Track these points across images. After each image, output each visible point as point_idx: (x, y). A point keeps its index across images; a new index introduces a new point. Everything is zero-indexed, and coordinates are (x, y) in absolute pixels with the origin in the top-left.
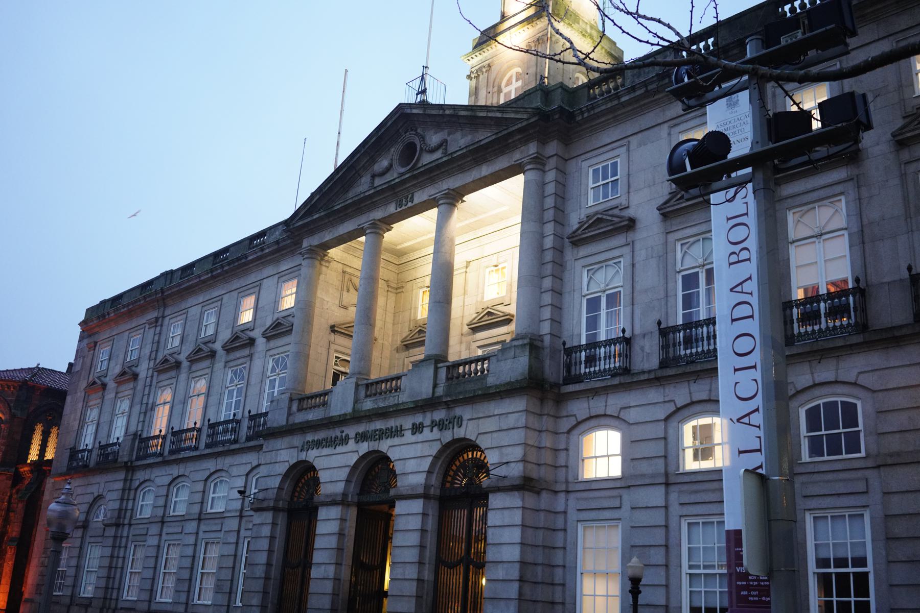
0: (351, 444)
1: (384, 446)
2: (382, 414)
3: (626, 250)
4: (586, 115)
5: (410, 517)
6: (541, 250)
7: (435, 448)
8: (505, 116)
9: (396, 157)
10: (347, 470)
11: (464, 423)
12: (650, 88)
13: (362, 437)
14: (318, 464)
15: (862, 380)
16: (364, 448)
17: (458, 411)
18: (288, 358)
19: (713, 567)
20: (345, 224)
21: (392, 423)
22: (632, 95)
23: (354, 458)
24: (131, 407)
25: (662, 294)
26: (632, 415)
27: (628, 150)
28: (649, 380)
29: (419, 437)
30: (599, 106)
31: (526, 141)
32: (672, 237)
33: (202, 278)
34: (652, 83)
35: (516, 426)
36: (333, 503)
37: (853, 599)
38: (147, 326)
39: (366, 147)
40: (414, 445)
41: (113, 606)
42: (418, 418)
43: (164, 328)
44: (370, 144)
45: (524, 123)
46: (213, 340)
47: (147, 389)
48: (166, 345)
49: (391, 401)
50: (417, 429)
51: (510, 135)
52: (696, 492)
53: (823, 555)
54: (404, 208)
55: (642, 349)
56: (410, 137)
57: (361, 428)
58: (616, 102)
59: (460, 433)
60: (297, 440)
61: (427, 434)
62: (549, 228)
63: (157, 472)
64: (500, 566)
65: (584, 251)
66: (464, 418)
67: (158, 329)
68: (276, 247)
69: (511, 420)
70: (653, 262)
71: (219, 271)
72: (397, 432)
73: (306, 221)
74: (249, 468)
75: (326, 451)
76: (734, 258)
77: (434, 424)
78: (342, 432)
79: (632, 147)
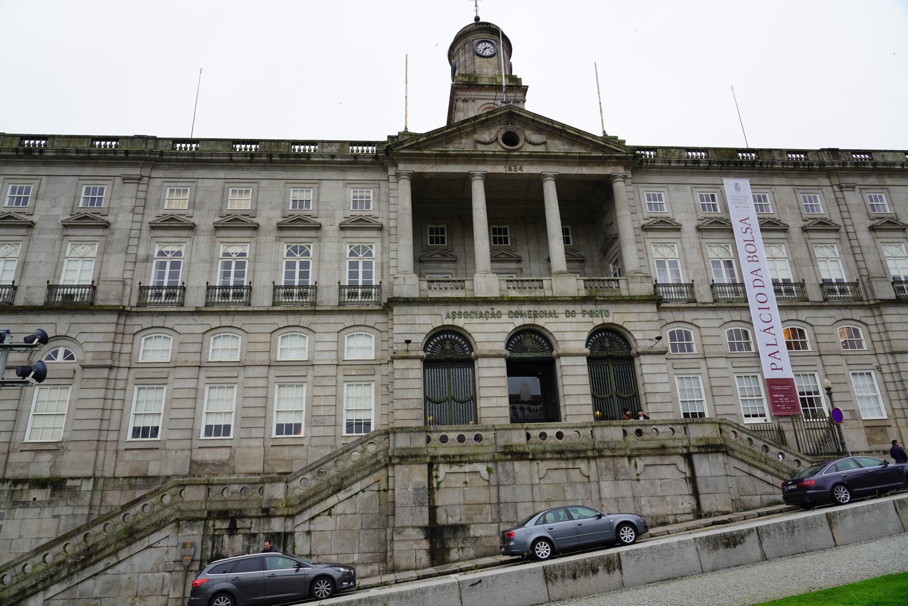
0: (505, 318)
1: (540, 322)
3: (678, 241)
4: (649, 164)
5: (577, 367)
7: (590, 328)
8: (607, 145)
9: (500, 138)
10: (506, 335)
11: (611, 315)
12: (688, 165)
13: (511, 314)
14: (468, 328)
15: (808, 320)
16: (519, 322)
17: (605, 307)
18: (290, 246)
19: (746, 396)
20: (451, 166)
22: (677, 165)
23: (511, 328)
24: (103, 252)
25: (704, 268)
26: (700, 323)
27: (668, 190)
28: (710, 307)
29: (574, 319)
30: (658, 162)
31: (617, 164)
33: (196, 158)
34: (689, 163)
35: (652, 320)
37: (809, 408)
39: (476, 121)
40: (569, 324)
41: (111, 447)
42: (571, 308)
43: (151, 188)
44: (479, 120)
45: (624, 155)
47: (134, 242)
48: (159, 203)
49: (538, 293)
50: (568, 314)
51: (610, 158)
52: (741, 362)
53: (801, 391)
54: (513, 172)
55: (699, 291)
56: (510, 128)
57: (514, 308)
58: (667, 164)
59: (609, 320)
60: (443, 310)
63: (171, 322)
64: (657, 395)
65: (650, 234)
66: (610, 311)
67: (142, 187)
68: (353, 159)
69: (648, 317)
70: (695, 251)
71: (265, 158)
72: (553, 314)
73: (411, 152)
74: (341, 327)
75: (475, 320)
76: (750, 259)
77: (584, 313)
78: (493, 309)
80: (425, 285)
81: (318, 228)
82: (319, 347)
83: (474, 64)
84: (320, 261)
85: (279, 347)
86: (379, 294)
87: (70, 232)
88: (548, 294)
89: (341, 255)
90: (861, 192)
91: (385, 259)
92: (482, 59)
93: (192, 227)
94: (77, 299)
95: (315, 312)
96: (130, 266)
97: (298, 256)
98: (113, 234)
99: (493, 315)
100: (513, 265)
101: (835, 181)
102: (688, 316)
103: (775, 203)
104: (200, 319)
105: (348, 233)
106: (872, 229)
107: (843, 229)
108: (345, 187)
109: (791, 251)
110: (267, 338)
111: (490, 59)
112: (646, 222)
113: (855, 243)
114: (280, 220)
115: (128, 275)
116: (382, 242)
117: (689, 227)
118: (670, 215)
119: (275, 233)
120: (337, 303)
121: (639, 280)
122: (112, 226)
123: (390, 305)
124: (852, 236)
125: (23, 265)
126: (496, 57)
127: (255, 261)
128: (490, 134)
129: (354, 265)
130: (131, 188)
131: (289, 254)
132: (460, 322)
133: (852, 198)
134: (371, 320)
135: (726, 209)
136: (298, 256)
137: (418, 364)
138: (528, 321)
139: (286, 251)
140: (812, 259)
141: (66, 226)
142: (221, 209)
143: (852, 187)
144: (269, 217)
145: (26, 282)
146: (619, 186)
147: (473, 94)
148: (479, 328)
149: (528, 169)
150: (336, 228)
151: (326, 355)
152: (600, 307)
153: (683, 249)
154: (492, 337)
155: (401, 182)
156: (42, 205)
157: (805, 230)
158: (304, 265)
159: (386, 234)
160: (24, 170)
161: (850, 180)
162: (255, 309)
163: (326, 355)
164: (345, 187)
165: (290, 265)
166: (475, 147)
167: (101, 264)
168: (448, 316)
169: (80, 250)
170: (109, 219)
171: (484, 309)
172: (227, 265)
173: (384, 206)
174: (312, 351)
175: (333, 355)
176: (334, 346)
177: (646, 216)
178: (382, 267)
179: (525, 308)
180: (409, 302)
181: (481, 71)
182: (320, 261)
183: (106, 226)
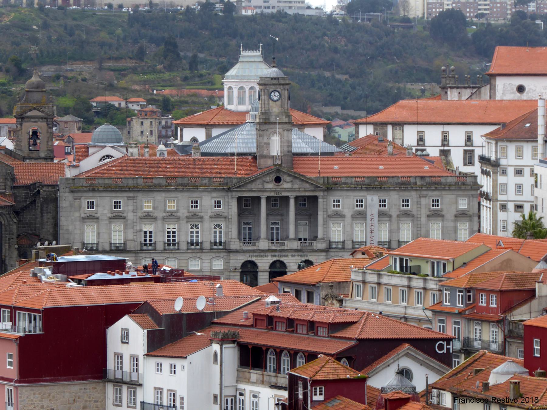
0: (269, 257)
1: (282, 259)
2: (281, 251)
6: (324, 218)
9: (274, 179)
14: (256, 261)
21: (284, 254)
23: (271, 261)
24: (125, 228)
27: (343, 199)
32: (354, 221)
36: (266, 271)
38: (126, 198)
42: (294, 254)
46: (177, 211)
47: (135, 224)
48: (142, 208)
49: (282, 248)
50: (293, 256)
57: (273, 254)
59: (307, 258)
60: (248, 254)
61: (296, 257)
62: (325, 213)
65: (332, 219)
67: (135, 201)
74: (211, 257)
75: (259, 258)
77: (298, 256)
79: (344, 198)
80: (242, 244)
81: (202, 218)
82: (204, 265)
83: (269, 104)
85: (190, 264)
86: (225, 246)
87: (112, 220)
88: (286, 248)
89: (210, 230)
90: (429, 198)
91: (227, 230)
92: (273, 102)
93: (155, 218)
94: (120, 248)
95: (202, 252)
96: (135, 234)
97: (195, 228)
98: (127, 221)
99: (265, 256)
100: (279, 217)
101: (419, 193)
103: (389, 204)
104: (162, 254)
105: (213, 219)
106: (428, 216)
107: (416, 216)
108: (211, 199)
109: (390, 226)
110: (185, 261)
111: (277, 103)
112: (331, 213)
113: (419, 223)
114: (187, 214)
115: (135, 237)
116: (226, 223)
118: (342, 210)
119: (186, 220)
120: (209, 249)
121: (321, 242)
122: (127, 218)
123: (230, 251)
124: (419, 219)
125: (99, 234)
126: (280, 100)
127: (179, 231)
128: (270, 177)
129: (215, 232)
130: (131, 202)
131: (191, 228)
132: (253, 259)
133: (424, 201)
134: (222, 255)
135: (366, 207)
136: (195, 228)
137: (239, 274)
138: (278, 259)
139: (190, 227)
140: (399, 229)
141: (110, 218)
142: (165, 210)
143: (425, 196)
144: (183, 213)
145: (101, 241)
146: (320, 200)
147: (267, 126)
148: (260, 261)
149: (284, 194)
150: (209, 217)
151: (206, 268)
152: (304, 254)
153: (345, 225)
154: (265, 265)
155: (233, 200)
156: (100, 209)
157: (398, 216)
158: (197, 232)
159: (227, 219)
160: (90, 195)
161: (425, 193)
162: (182, 251)
163: (206, 268)
164: (211, 199)
165: (192, 232)
166: (263, 185)
167: (125, 233)
168: (249, 257)
169: (117, 228)
170: (125, 215)
171: (262, 254)
172: (169, 233)
173: (226, 207)
174: (202, 266)
175: (209, 268)
176: (209, 265)
177: (331, 210)
178: (226, 234)
179: (277, 254)
180: (237, 251)
181: (272, 110)
183: (124, 218)
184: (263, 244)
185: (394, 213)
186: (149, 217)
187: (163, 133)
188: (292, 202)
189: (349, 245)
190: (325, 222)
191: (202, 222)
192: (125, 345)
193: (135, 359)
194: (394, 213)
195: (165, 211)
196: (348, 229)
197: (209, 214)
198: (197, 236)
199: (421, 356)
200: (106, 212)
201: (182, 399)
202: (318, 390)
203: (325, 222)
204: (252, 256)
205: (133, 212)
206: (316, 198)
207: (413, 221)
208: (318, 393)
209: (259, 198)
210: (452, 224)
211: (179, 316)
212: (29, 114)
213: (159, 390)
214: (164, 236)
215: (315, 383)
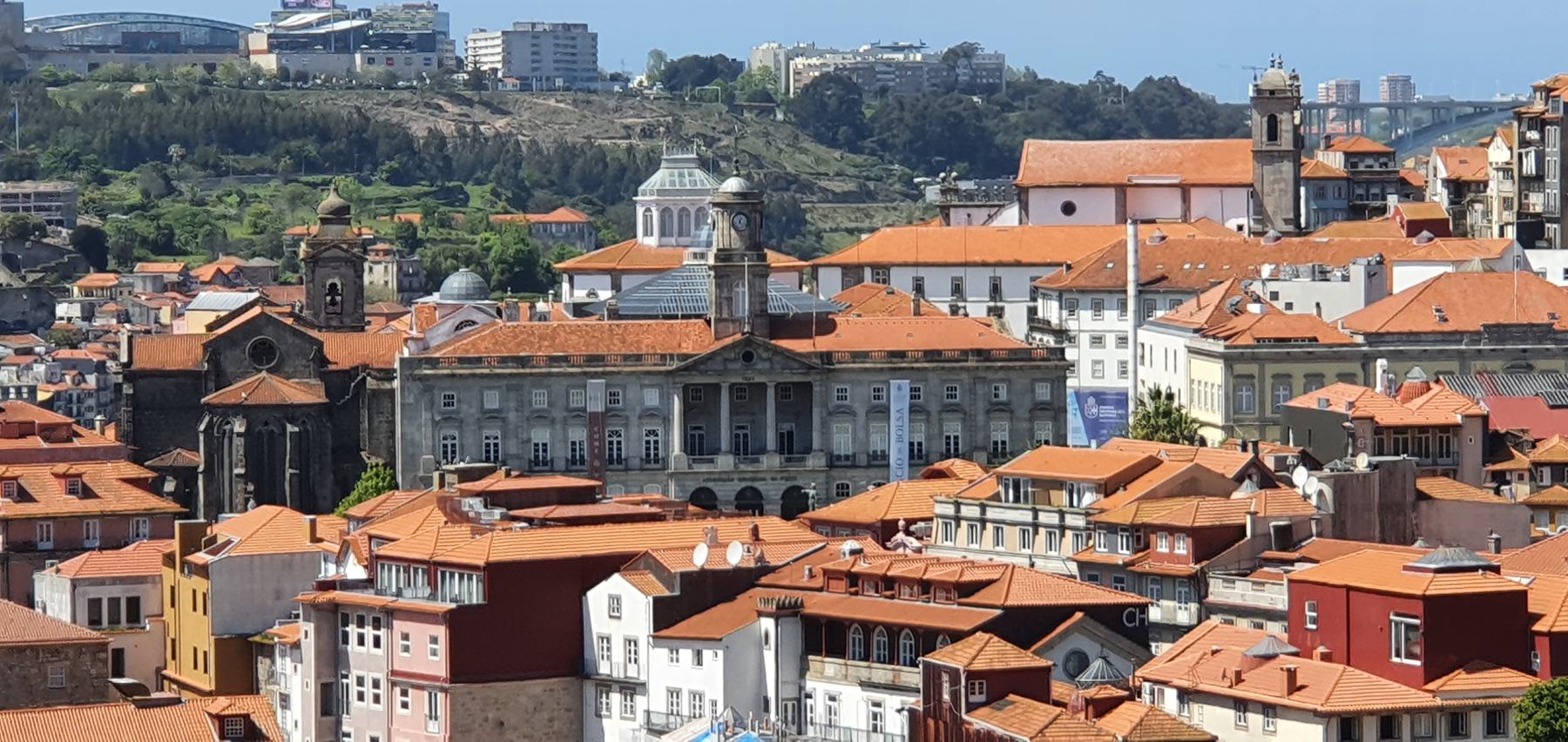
1: (757, 485)
16: (744, 484)
48: (530, 403)
50: (773, 479)
72: (764, 479)
84: (628, 439)
89: (640, 439)
102: (850, 473)
103: (925, 392)
106: (988, 412)
117: (861, 412)
130: (512, 395)
132: (710, 485)
138: (749, 484)
146: (816, 389)
156: (464, 407)
157: (940, 412)
171: (724, 476)
182: (628, 439)
184: (725, 462)
185: (934, 407)
186: (541, 417)
187: (406, 283)
188: (771, 393)
189: (862, 460)
190: (825, 425)
191: (626, 425)
192: (615, 622)
193: (631, 642)
194: (934, 407)
195: (568, 409)
196: (861, 435)
197: (638, 413)
198: (619, 449)
199: (1102, 631)
200: (473, 410)
201: (714, 703)
202: (977, 686)
203: (825, 425)
204: (706, 480)
205: (517, 410)
206: (809, 385)
207: (964, 420)
208: (977, 691)
209: (716, 388)
210: (1026, 425)
211: (703, 573)
212: (326, 254)
213: (674, 693)
214: (567, 448)
215: (972, 675)
